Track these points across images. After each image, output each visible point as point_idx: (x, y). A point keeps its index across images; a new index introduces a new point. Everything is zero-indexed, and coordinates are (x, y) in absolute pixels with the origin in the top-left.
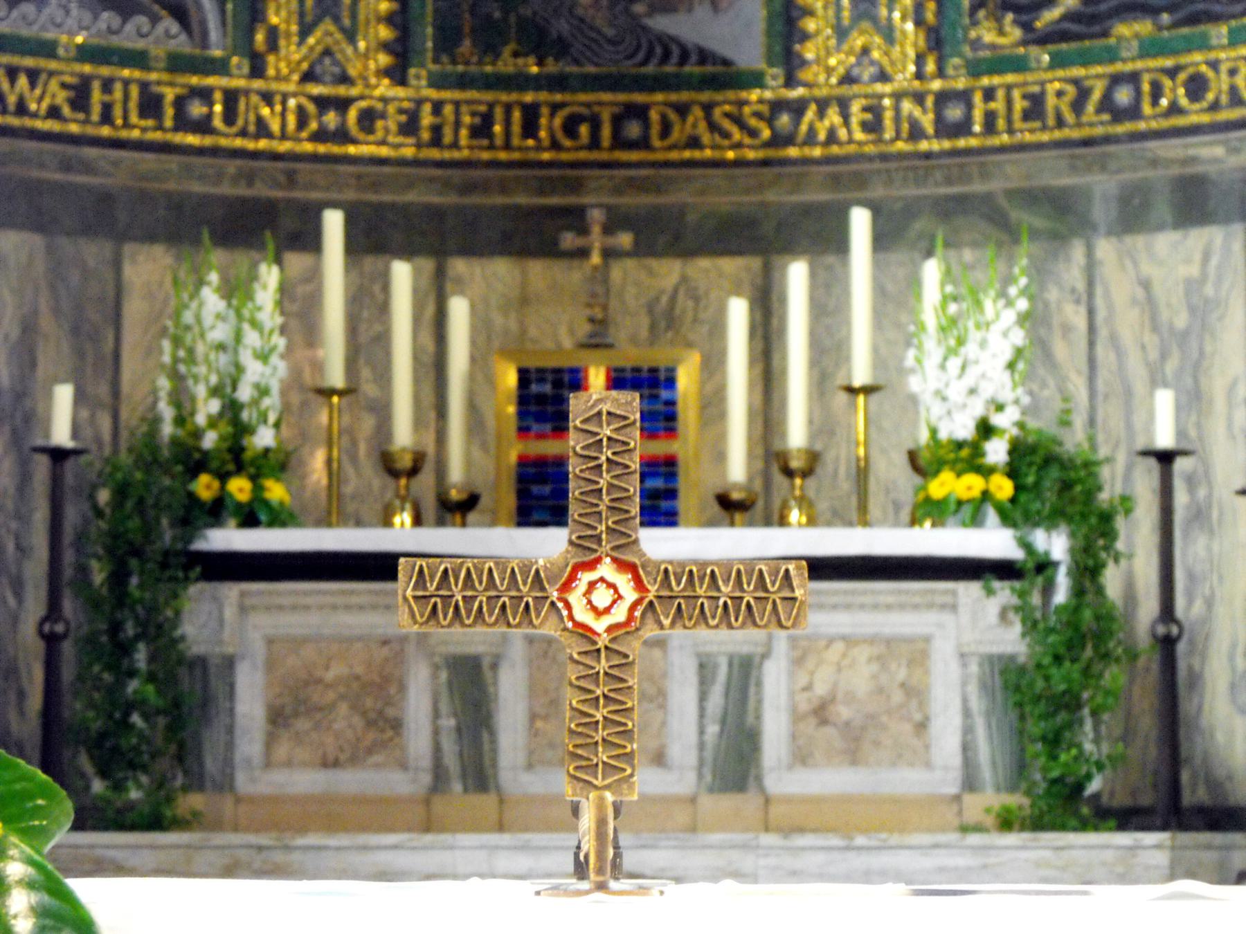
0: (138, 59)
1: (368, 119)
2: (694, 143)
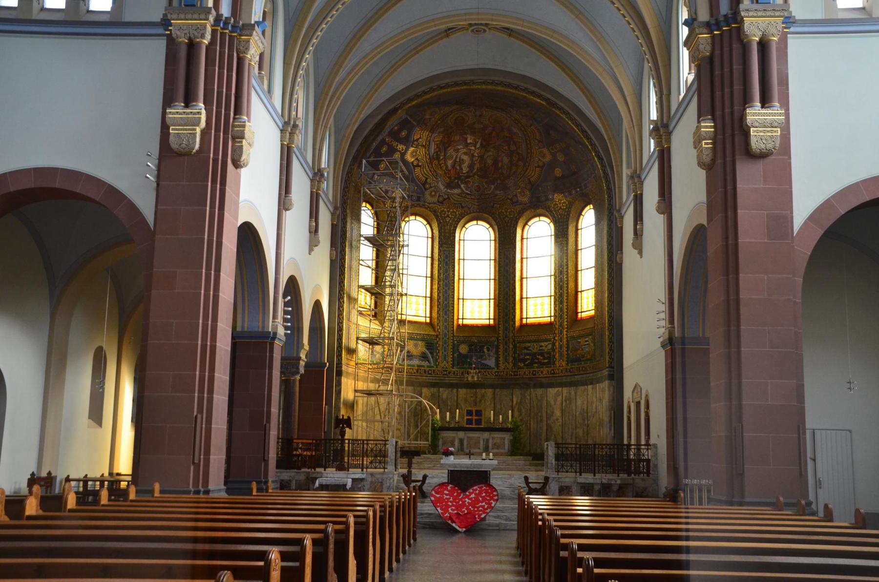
1: (449, 373)
2: (486, 376)
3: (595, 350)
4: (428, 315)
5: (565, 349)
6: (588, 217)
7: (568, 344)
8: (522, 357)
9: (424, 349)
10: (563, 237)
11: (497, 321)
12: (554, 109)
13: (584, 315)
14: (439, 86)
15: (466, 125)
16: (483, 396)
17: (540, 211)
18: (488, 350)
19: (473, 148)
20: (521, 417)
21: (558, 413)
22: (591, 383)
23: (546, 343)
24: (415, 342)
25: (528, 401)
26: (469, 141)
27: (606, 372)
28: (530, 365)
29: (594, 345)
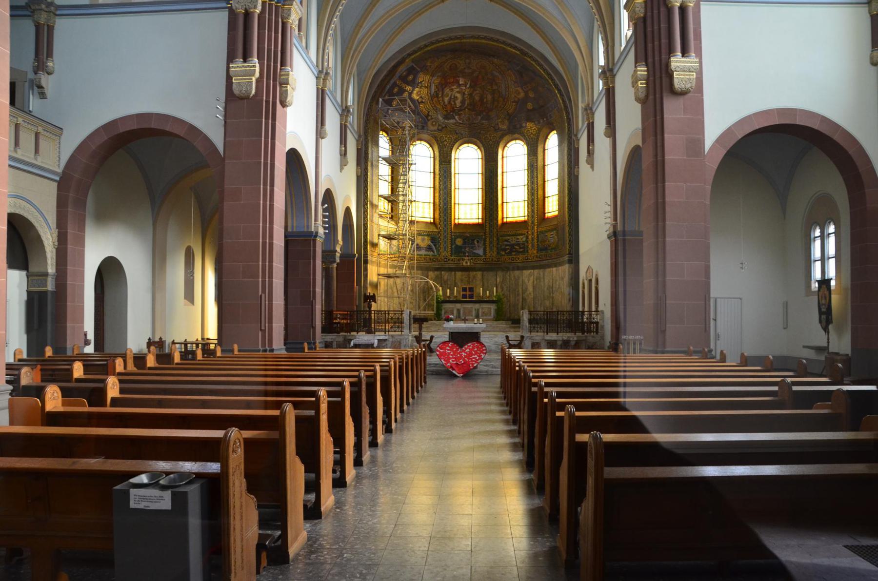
0: (429, 255)
1: (449, 260)
2: (476, 262)
3: (558, 241)
4: (432, 216)
5: (536, 241)
6: (553, 140)
7: (538, 237)
8: (503, 247)
9: (430, 243)
10: (534, 156)
11: (484, 220)
12: (526, 57)
13: (550, 215)
14: (437, 40)
16: (474, 277)
17: (516, 136)
18: (478, 242)
19: (464, 88)
20: (503, 293)
21: (530, 289)
22: (556, 266)
23: (522, 237)
24: (423, 237)
25: (508, 281)
26: (461, 83)
27: (566, 258)
28: (510, 253)
29: (558, 238)
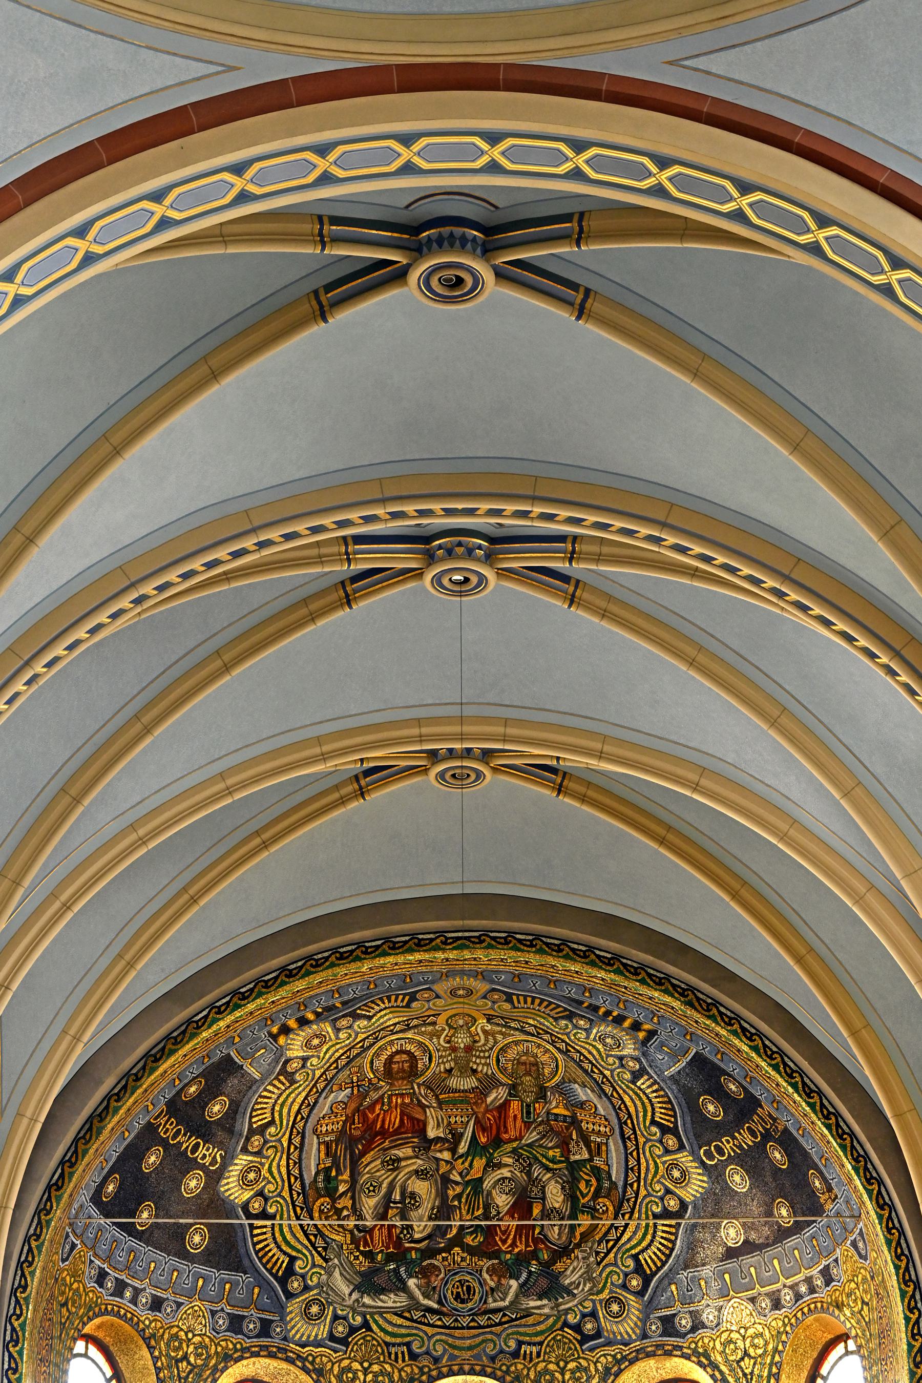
15: (421, 1080)
19: (446, 1155)
26: (431, 1133)
